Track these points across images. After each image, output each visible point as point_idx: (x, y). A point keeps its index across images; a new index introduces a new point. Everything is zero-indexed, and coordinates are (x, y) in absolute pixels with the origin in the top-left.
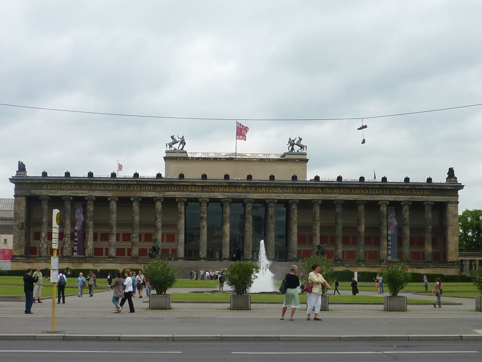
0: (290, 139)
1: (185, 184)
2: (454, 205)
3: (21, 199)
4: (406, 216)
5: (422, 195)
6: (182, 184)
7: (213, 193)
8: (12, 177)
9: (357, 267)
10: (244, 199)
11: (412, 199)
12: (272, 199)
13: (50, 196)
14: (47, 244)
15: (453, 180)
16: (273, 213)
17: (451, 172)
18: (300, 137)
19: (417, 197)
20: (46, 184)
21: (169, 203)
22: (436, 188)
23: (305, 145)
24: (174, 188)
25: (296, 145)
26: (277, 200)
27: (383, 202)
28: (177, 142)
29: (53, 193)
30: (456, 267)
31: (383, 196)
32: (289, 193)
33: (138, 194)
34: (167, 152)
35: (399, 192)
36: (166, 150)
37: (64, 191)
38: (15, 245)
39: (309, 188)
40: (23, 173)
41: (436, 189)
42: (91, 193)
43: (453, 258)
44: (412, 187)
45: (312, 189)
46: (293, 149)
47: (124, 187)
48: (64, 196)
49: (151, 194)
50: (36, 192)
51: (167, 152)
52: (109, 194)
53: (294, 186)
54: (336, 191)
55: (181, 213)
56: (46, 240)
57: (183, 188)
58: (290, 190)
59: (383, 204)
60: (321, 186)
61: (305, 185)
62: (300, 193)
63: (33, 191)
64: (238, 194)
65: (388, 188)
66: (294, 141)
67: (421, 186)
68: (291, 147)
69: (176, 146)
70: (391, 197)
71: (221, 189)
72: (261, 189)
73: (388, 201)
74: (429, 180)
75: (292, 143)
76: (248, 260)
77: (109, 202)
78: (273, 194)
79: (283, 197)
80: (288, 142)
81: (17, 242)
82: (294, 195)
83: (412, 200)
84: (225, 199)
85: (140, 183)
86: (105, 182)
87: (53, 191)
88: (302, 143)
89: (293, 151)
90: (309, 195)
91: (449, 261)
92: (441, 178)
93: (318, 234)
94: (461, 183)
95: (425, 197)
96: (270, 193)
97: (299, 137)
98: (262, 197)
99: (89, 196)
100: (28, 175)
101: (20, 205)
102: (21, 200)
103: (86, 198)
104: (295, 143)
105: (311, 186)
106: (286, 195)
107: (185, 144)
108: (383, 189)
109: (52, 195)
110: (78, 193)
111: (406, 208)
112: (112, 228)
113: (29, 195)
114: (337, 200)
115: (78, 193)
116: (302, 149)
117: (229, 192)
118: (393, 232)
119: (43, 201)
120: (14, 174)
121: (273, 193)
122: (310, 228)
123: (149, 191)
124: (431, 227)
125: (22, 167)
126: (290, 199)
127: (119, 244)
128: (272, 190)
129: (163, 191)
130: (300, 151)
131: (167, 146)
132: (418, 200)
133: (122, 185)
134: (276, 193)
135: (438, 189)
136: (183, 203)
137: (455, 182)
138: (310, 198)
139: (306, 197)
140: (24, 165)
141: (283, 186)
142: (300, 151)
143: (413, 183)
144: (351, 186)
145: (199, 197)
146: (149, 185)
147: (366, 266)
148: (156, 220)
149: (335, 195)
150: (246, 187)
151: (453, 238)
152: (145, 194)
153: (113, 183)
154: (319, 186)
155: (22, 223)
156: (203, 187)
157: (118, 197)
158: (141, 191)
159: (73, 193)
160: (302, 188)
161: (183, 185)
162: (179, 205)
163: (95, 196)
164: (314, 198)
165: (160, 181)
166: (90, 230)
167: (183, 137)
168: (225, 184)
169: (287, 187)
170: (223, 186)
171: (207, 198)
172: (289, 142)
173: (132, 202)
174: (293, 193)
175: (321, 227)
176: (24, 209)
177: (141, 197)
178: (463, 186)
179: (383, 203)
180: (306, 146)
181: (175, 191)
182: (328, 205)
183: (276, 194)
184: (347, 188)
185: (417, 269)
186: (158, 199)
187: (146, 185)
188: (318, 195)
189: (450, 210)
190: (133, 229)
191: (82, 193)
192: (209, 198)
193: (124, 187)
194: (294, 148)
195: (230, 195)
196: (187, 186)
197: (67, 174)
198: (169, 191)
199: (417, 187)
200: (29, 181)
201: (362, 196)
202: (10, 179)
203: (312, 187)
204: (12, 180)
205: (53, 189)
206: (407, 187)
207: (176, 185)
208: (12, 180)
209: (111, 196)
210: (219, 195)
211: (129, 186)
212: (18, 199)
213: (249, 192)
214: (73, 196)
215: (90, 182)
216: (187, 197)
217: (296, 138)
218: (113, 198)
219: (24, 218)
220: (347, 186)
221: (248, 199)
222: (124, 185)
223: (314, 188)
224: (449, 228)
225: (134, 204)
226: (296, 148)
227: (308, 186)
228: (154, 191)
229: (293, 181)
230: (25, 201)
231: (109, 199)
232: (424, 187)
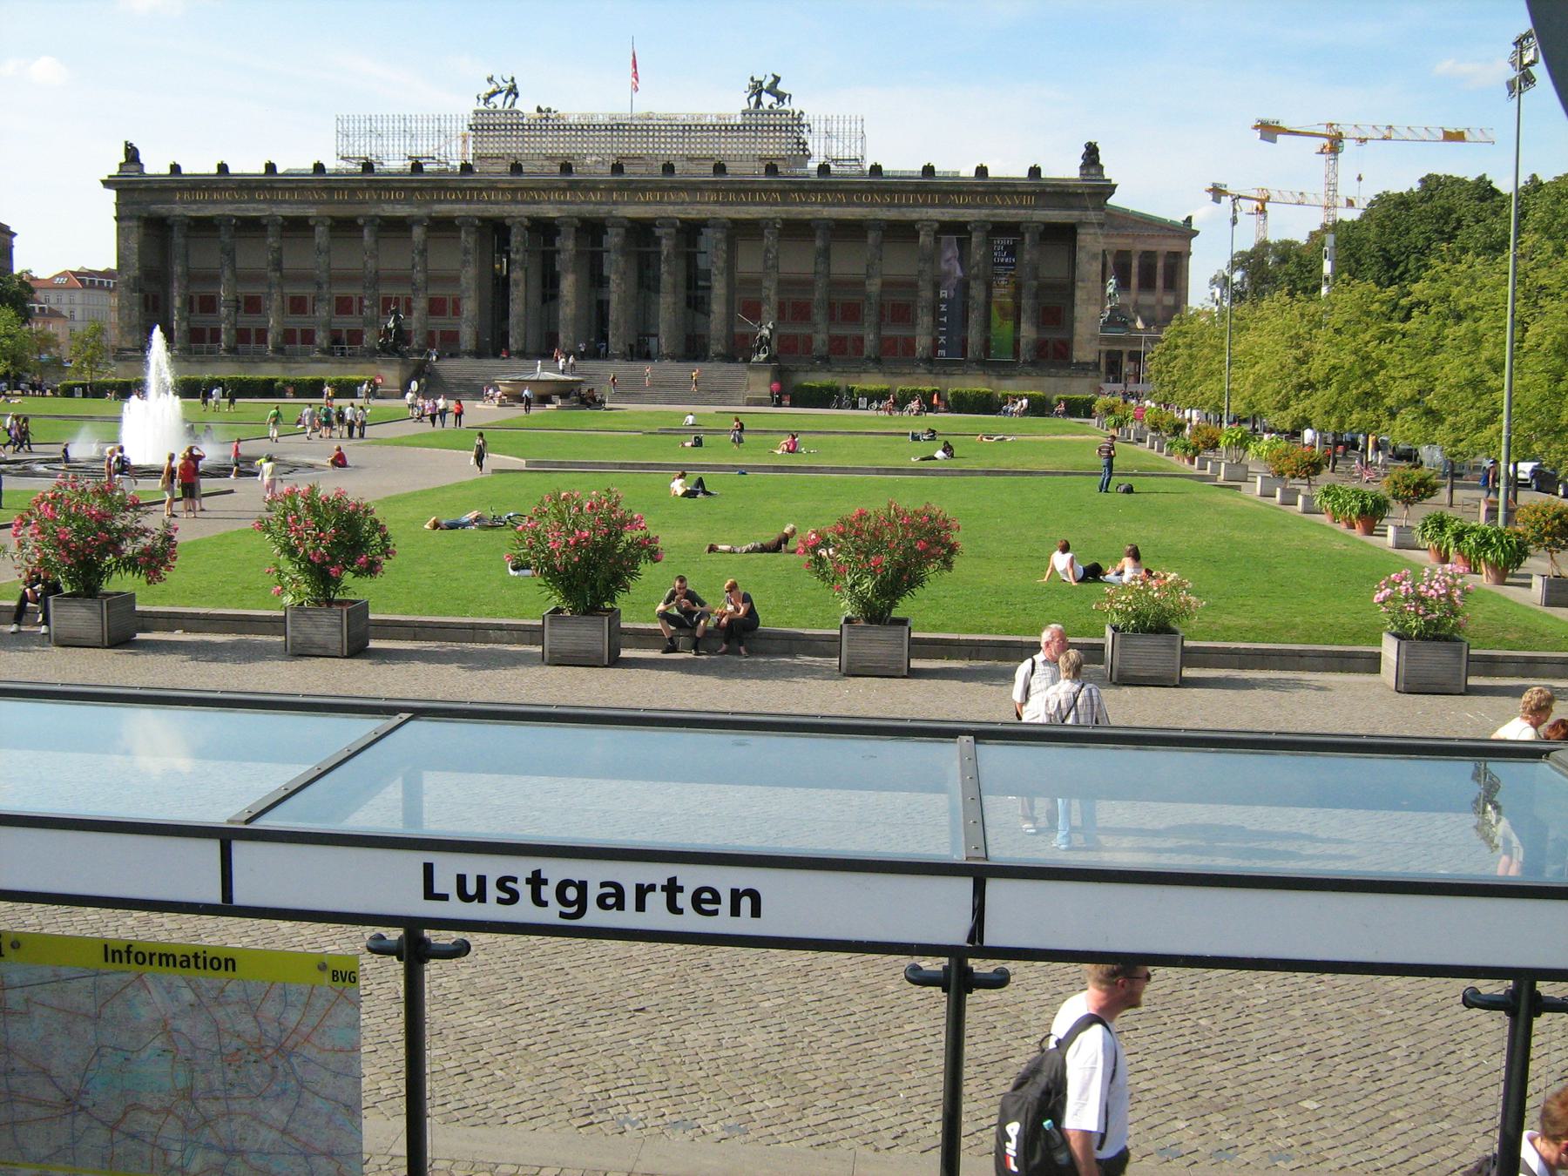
0: (752, 79)
1: (473, 185)
2: (1092, 231)
3: (131, 224)
4: (978, 257)
5: (1014, 207)
6: (465, 185)
7: (535, 206)
8: (110, 176)
9: (862, 375)
10: (605, 219)
11: (994, 216)
12: (669, 218)
13: (191, 217)
14: (188, 322)
15: (1093, 171)
16: (671, 251)
17: (1091, 154)
18: (776, 74)
19: (1005, 211)
20: (179, 189)
21: (443, 226)
22: (1048, 189)
24: (451, 196)
25: (768, 91)
26: (682, 221)
27: (925, 223)
28: (501, 92)
29: (194, 211)
30: (1090, 374)
31: (925, 210)
32: (708, 203)
33: (373, 211)
34: (476, 113)
35: (964, 200)
36: (477, 108)
37: (218, 206)
38: (121, 325)
39: (754, 191)
40: (133, 167)
41: (1049, 193)
42: (274, 210)
43: (1085, 356)
44: (991, 189)
46: (759, 103)
47: (343, 194)
48: (219, 215)
49: (402, 211)
50: (160, 209)
51: (476, 113)
52: (311, 211)
53: (718, 187)
54: (816, 199)
55: (466, 252)
56: (186, 314)
57: (472, 196)
58: (709, 198)
59: (925, 229)
60: (780, 187)
61: (742, 186)
62: (732, 204)
63: (153, 206)
64: (591, 207)
65: (937, 192)
66: (761, 83)
67: (1014, 185)
68: (755, 97)
69: (498, 100)
70: (943, 213)
71: (555, 196)
72: (645, 197)
73: (937, 221)
74: (1035, 172)
75: (757, 90)
76: (615, 356)
77: (312, 229)
78: (671, 207)
79: (694, 212)
81: (127, 317)
82: (717, 208)
83: (992, 219)
84: (564, 220)
85: (374, 185)
86: (301, 185)
87: (195, 207)
88: (780, 87)
89: (761, 108)
90: (754, 208)
91: (1075, 361)
92: (1064, 167)
93: (773, 298)
94: (1110, 180)
95: (1023, 211)
97: (773, 75)
98: (646, 212)
99: (270, 216)
100: (149, 169)
101: (126, 240)
102: (129, 227)
103: (264, 221)
104: (765, 85)
105: (756, 186)
106: (704, 207)
107: (517, 95)
108: (927, 193)
109: (193, 214)
110: (248, 210)
111: (976, 238)
112: (320, 286)
113: (145, 215)
114: (819, 219)
115: (248, 210)
117: (572, 203)
118: (952, 294)
119: (176, 228)
120: (115, 171)
121: (670, 203)
122: (756, 283)
123: (398, 202)
124: (1035, 283)
125: (132, 154)
126: (708, 219)
127: (352, 320)
128: (669, 196)
129: (427, 203)
130: (775, 107)
131: (478, 99)
132: (1008, 219)
133: (338, 189)
135: (1059, 193)
136: (473, 229)
137: (1098, 177)
138: (755, 216)
139: (747, 213)
140: (136, 151)
143: (995, 178)
144: (848, 187)
145: (505, 214)
146: (395, 189)
147: (880, 371)
148: (413, 267)
149: (815, 208)
150: (610, 190)
151: (1087, 309)
152: (388, 210)
153: (318, 185)
154: (775, 186)
155: (135, 278)
156: (515, 190)
157: (332, 218)
158: (379, 201)
159: (237, 210)
160: (738, 192)
161: (471, 189)
162: (463, 235)
163: (285, 218)
164: (764, 216)
165: (418, 181)
166: (273, 291)
167: (513, 80)
168: (562, 185)
169: (700, 190)
170: (559, 189)
171: (521, 216)
173: (360, 229)
174: (716, 202)
175: (780, 283)
176: (136, 246)
177: (381, 218)
178: (1115, 186)
179: (923, 226)
181: (452, 202)
182: (796, 230)
183: (677, 207)
184: (841, 191)
185: (999, 379)
186: (418, 221)
187: (389, 190)
189: (1082, 244)
190: (364, 287)
191: (254, 210)
192: (529, 218)
193: (343, 194)
194: (762, 100)
195: (574, 209)
196: (480, 190)
197: (223, 168)
198: (440, 201)
199: (1002, 189)
200: (143, 186)
201: (877, 209)
203: (760, 191)
204: (107, 184)
205: (195, 202)
206: (980, 189)
207: (455, 189)
208: (107, 184)
209: (315, 214)
210: (550, 211)
211: (353, 191)
212: (124, 224)
213: (615, 203)
214: (235, 217)
215: (268, 185)
216: (479, 214)
218: (320, 219)
219: (137, 265)
220: (840, 187)
221: (616, 217)
222: (343, 189)
223: (765, 191)
224: (1080, 284)
225: (366, 232)
226: (767, 99)
227: (749, 186)
228: (407, 201)
229: (714, 176)
230: (141, 230)
231: (312, 222)
232: (1020, 189)
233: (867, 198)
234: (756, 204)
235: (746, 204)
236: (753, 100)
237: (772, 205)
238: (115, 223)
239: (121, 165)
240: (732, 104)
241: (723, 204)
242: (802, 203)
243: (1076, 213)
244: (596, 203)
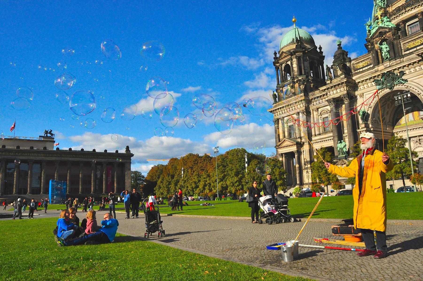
2: (129, 164)
19: (110, 160)
32: (41, 156)
45: (55, 155)
54: (68, 156)
58: (42, 155)
62: (48, 157)
64: (10, 156)
78: (32, 157)
95: (114, 160)
96: (30, 156)
134: (34, 156)
141: (38, 152)
174: (43, 156)
188: (58, 158)
206: (106, 155)
213: (17, 156)
233: (80, 156)
234: (53, 157)
235: (51, 157)
237: (57, 157)
241: (45, 157)
242: (65, 157)
243: (125, 160)
244: (12, 155)
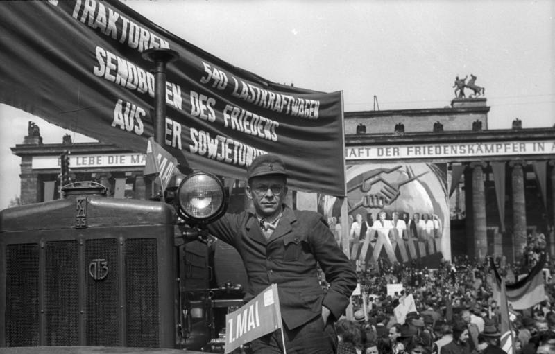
0: (457, 78)
18: (474, 75)
23: (481, 86)
25: (467, 87)
46: (462, 93)
66: (463, 81)
75: (460, 84)
80: (454, 85)
88: (477, 83)
89: (463, 97)
97: (472, 75)
104: (466, 82)
116: (477, 94)
120: (21, 142)
140: (37, 127)
142: (473, 97)
172: (456, 83)
180: (484, 89)
202: (13, 149)
217: (467, 77)
226: (468, 92)
236: (459, 92)
238: (20, 179)
239: (26, 138)
240: (443, 97)
